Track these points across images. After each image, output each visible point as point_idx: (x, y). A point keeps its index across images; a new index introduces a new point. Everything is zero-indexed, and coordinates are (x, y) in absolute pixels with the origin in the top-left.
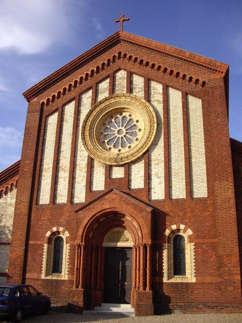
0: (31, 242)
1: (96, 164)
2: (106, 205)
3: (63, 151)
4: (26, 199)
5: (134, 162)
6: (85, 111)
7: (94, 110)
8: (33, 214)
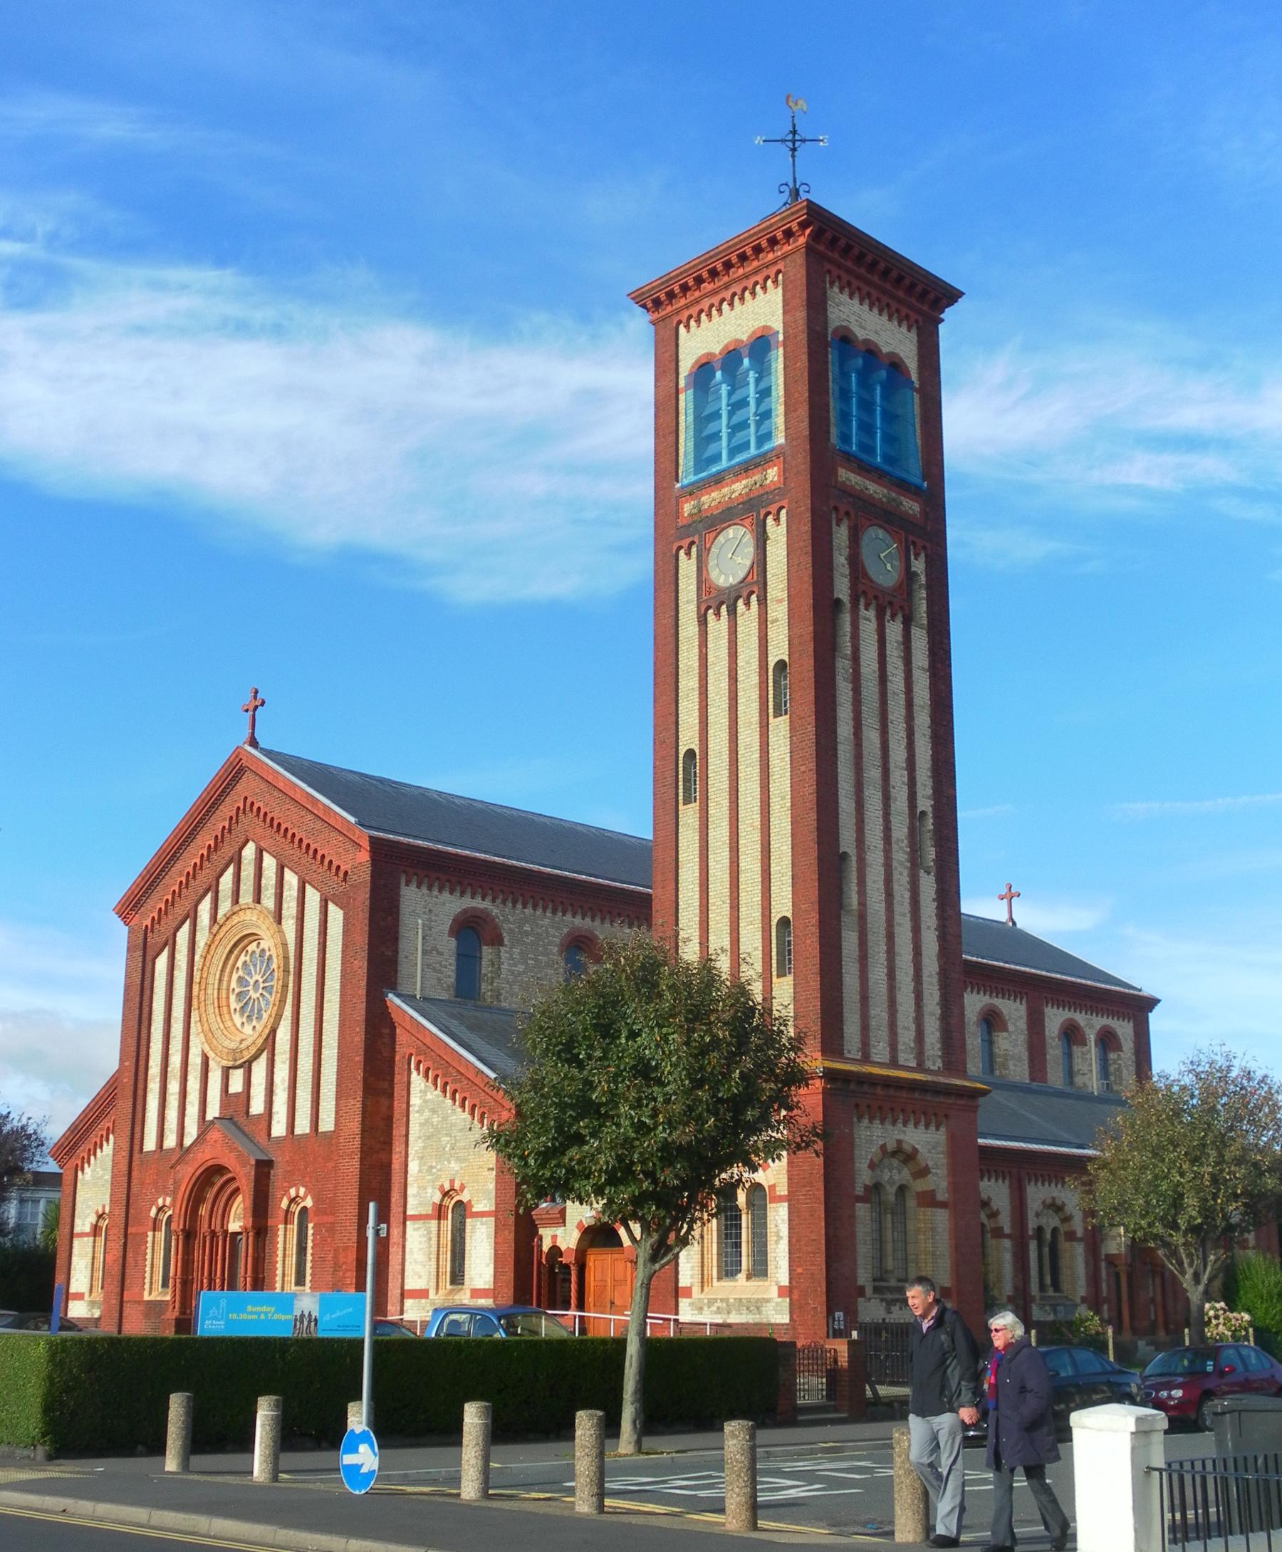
0: (130, 1230)
1: (211, 1063)
2: (206, 1156)
3: (175, 1037)
4: (126, 1146)
5: (256, 1057)
6: (202, 939)
7: (213, 941)
8: (134, 1173)
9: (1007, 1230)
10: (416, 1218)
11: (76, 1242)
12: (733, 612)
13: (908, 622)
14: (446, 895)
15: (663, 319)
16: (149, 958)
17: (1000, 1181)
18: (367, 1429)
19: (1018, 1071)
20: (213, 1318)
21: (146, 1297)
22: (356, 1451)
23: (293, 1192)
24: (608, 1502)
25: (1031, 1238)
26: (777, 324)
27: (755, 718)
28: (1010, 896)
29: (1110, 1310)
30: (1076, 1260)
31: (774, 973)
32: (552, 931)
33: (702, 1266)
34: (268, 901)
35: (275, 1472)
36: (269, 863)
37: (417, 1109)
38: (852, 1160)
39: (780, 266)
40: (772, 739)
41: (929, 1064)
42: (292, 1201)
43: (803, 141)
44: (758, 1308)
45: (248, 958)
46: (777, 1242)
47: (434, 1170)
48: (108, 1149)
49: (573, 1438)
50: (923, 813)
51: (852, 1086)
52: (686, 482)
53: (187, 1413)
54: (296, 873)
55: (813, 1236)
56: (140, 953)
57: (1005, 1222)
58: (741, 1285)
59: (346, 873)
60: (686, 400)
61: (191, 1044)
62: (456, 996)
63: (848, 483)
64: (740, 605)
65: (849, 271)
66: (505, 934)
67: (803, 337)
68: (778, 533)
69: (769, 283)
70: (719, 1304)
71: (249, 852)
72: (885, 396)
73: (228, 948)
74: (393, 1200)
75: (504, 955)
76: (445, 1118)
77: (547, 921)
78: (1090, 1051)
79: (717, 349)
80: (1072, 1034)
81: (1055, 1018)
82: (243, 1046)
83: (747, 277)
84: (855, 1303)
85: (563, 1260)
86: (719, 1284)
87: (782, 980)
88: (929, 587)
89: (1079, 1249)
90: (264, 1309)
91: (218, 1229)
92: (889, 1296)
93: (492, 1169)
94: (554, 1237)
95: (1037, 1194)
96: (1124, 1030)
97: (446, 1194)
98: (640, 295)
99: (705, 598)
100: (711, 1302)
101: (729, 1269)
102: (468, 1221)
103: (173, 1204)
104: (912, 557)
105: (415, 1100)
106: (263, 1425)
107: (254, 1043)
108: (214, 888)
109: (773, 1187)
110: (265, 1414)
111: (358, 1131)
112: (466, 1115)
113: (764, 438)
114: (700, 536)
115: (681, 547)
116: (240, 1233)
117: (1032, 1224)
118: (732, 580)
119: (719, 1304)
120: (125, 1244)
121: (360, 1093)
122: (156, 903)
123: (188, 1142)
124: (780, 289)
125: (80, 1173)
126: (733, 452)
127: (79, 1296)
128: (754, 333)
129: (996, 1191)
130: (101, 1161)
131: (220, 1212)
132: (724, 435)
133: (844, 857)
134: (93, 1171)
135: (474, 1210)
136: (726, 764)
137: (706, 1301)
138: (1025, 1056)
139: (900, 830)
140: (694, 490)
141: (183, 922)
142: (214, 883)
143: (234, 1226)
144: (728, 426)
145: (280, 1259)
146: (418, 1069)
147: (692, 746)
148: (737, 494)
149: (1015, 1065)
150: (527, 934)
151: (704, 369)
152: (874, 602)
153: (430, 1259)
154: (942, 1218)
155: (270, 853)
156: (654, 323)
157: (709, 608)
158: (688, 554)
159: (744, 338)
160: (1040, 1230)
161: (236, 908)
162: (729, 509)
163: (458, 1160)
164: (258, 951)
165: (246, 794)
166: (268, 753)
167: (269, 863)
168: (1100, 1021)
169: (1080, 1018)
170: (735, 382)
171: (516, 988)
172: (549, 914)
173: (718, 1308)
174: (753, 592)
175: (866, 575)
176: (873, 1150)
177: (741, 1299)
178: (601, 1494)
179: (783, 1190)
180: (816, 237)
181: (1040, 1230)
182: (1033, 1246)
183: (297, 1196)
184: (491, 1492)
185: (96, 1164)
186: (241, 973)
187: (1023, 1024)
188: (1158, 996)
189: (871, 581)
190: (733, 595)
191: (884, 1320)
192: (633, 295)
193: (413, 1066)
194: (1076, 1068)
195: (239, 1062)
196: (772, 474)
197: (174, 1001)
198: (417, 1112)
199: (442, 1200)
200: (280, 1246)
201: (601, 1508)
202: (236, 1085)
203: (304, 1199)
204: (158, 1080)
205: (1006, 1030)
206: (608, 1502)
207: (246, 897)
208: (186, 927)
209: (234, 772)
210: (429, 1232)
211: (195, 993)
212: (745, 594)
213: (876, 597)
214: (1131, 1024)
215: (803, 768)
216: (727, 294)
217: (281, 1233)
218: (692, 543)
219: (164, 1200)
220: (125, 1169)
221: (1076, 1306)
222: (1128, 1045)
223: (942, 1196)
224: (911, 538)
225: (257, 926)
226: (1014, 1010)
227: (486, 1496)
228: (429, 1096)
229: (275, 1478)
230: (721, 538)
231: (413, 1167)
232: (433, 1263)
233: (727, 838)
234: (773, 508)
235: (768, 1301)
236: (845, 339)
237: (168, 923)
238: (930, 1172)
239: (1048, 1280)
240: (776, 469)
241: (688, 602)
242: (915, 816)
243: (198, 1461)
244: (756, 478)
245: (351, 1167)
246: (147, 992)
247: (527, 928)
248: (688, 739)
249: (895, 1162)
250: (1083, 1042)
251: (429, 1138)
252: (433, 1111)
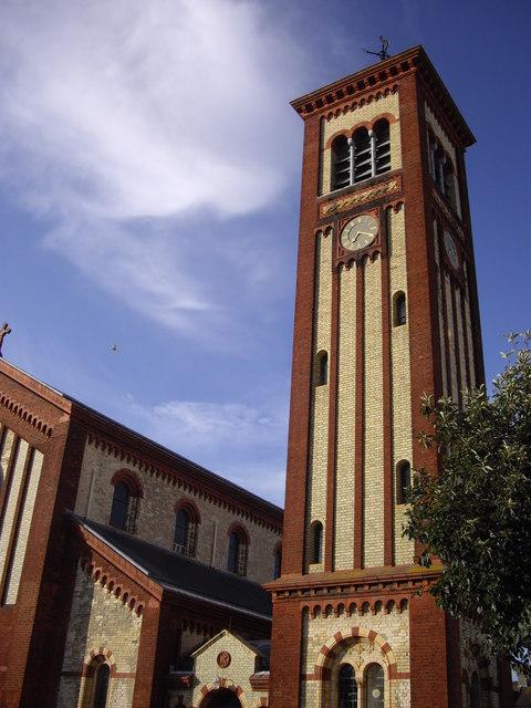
10: (66, 674)
12: (361, 265)
14: (112, 457)
32: (171, 496)
60: (327, 155)
68: (398, 221)
79: (349, 127)
93: (136, 642)
102: (112, 681)
111: (34, 605)
112: (119, 601)
121: (39, 577)
132: (351, 173)
140: (330, 199)
151: (339, 143)
163: (108, 633)
171: (147, 527)
193: (79, 563)
196: (392, 185)
212: (371, 253)
215: (421, 357)
230: (352, 224)
234: (393, 203)
248: (324, 344)
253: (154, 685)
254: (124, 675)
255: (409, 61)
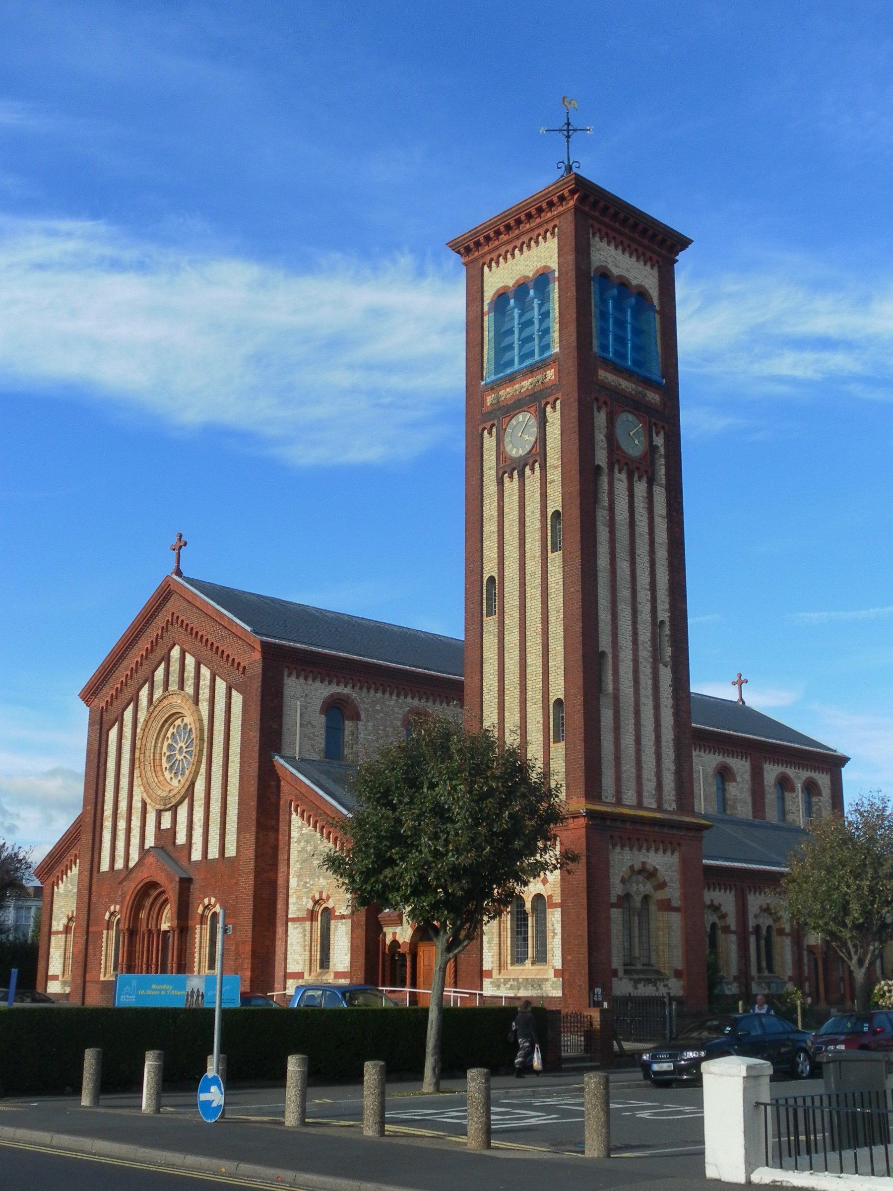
0: (92, 929)
1: (149, 807)
2: (144, 875)
3: (123, 788)
5: (180, 802)
6: (142, 716)
7: (149, 718)
8: (94, 888)
9: (733, 927)
10: (294, 920)
11: (53, 938)
12: (522, 476)
13: (651, 482)
15: (472, 262)
16: (104, 730)
17: (728, 892)
18: (216, 1075)
19: (744, 811)
20: (126, 994)
21: (102, 978)
22: (209, 1091)
23: (206, 901)
24: (387, 1127)
25: (752, 933)
26: (554, 266)
27: (538, 554)
28: (740, 682)
29: (810, 987)
30: (785, 950)
31: (552, 740)
32: (397, 710)
33: (500, 955)
34: (189, 689)
35: (158, 1107)
36: (190, 660)
37: (295, 840)
38: (607, 877)
39: (556, 222)
40: (550, 568)
41: (666, 806)
42: (206, 907)
43: (575, 130)
44: (539, 985)
45: (175, 730)
46: (553, 937)
47: (308, 885)
48: (75, 870)
49: (362, 1082)
50: (662, 622)
51: (608, 823)
52: (488, 380)
53: (97, 1064)
54: (209, 668)
55: (579, 933)
56: (98, 727)
57: (732, 921)
58: (528, 969)
59: (244, 668)
60: (488, 321)
61: (134, 793)
62: (326, 758)
63: (606, 380)
64: (528, 471)
65: (606, 225)
66: (362, 712)
67: (572, 274)
68: (554, 417)
69: (548, 234)
70: (512, 982)
71: (176, 652)
72: (634, 317)
73: (161, 723)
74: (279, 907)
75: (360, 726)
76: (316, 847)
77: (392, 703)
78: (797, 797)
79: (511, 283)
80: (784, 783)
81: (771, 772)
82: (171, 795)
83: (532, 230)
84: (611, 982)
85: (401, 950)
86: (512, 968)
87: (556, 745)
88: (667, 456)
89: (787, 941)
90: (164, 987)
91: (153, 928)
92: (636, 977)
94: (394, 934)
95: (755, 902)
96: (823, 780)
97: (316, 903)
98: (455, 244)
99: (502, 465)
100: (506, 981)
101: (519, 958)
102: (332, 922)
103: (121, 911)
104: (654, 434)
105: (295, 834)
106: (149, 1072)
107: (179, 792)
108: (151, 679)
109: (550, 897)
110: (150, 1064)
113: (545, 348)
114: (499, 419)
115: (484, 429)
116: (168, 931)
117: (752, 923)
118: (521, 452)
119: (512, 982)
120: (87, 939)
121: (254, 828)
122: (109, 691)
123: (132, 864)
124: (556, 238)
125: (55, 888)
126: (522, 358)
127: (55, 978)
128: (538, 271)
129: (726, 900)
130: (71, 879)
131: (155, 916)
133: (603, 654)
134: (66, 886)
135: (337, 914)
136: (517, 587)
137: (502, 980)
138: (749, 800)
139: (645, 635)
140: (494, 387)
141: (128, 705)
142: (150, 676)
143: (165, 926)
144: (519, 340)
145: (197, 950)
146: (296, 811)
147: (493, 574)
148: (525, 389)
149: (742, 807)
150: (378, 712)
151: (502, 297)
152: (625, 468)
153: (305, 951)
154: (676, 919)
155: (190, 653)
156: (465, 264)
157: (505, 472)
158: (490, 433)
159: (531, 275)
160: (758, 928)
161: (167, 694)
162: (519, 400)
164: (182, 725)
165: (173, 610)
166: (190, 581)
167: (190, 660)
168: (805, 774)
169: (791, 772)
170: (524, 307)
172: (394, 697)
173: (511, 985)
174: (536, 461)
175: (619, 448)
176: (624, 869)
177: (527, 979)
178: (382, 1122)
179: (557, 899)
180: (582, 200)
181: (758, 928)
182: (752, 939)
183: (210, 904)
184: (307, 1120)
185: (67, 881)
186: (170, 741)
187: (747, 777)
188: (848, 756)
189: (624, 452)
190: (522, 463)
191: (630, 994)
192: (451, 244)
193: (293, 809)
194: (787, 808)
195: (168, 806)
196: (550, 374)
197: (122, 762)
198: (296, 842)
199: (314, 907)
200: (197, 941)
201: (382, 1132)
202: (166, 824)
203: (214, 906)
204: (110, 819)
205: (735, 781)
206: (387, 1127)
207: (173, 687)
208: (131, 708)
209: (165, 594)
210: (305, 930)
211: (137, 756)
212: (531, 462)
213: (626, 464)
214: (829, 776)
215: (572, 590)
216: (518, 243)
217: (198, 931)
218: (493, 425)
219: (115, 907)
220: (87, 885)
221: (785, 983)
222: (826, 791)
223: (676, 903)
224: (653, 420)
225: (182, 707)
226: (741, 766)
227: (303, 1123)
228: (304, 831)
229: (158, 1110)
230: (514, 422)
231: (293, 882)
232: (307, 953)
233: (518, 641)
234: (551, 400)
235: (547, 980)
236: (604, 275)
237: (118, 705)
238: (667, 886)
239: (764, 964)
240: (553, 370)
241: (490, 468)
242: (656, 625)
243: (106, 1099)
244: (539, 377)
245: (247, 882)
246: (103, 756)
247: (378, 707)
248: (490, 569)
249: (641, 878)
250: (793, 789)
251: (304, 861)
252: (308, 842)
253: (367, 925)
254: (343, 917)
255: (566, 193)
